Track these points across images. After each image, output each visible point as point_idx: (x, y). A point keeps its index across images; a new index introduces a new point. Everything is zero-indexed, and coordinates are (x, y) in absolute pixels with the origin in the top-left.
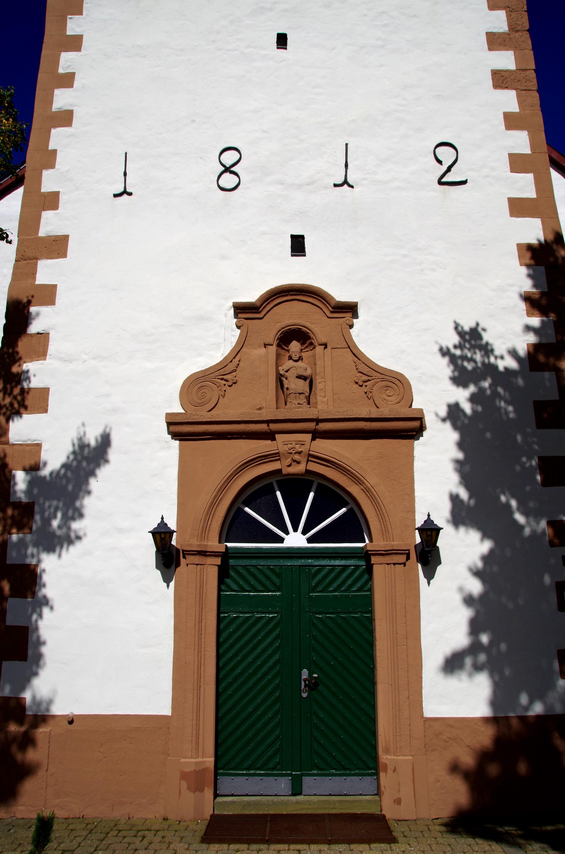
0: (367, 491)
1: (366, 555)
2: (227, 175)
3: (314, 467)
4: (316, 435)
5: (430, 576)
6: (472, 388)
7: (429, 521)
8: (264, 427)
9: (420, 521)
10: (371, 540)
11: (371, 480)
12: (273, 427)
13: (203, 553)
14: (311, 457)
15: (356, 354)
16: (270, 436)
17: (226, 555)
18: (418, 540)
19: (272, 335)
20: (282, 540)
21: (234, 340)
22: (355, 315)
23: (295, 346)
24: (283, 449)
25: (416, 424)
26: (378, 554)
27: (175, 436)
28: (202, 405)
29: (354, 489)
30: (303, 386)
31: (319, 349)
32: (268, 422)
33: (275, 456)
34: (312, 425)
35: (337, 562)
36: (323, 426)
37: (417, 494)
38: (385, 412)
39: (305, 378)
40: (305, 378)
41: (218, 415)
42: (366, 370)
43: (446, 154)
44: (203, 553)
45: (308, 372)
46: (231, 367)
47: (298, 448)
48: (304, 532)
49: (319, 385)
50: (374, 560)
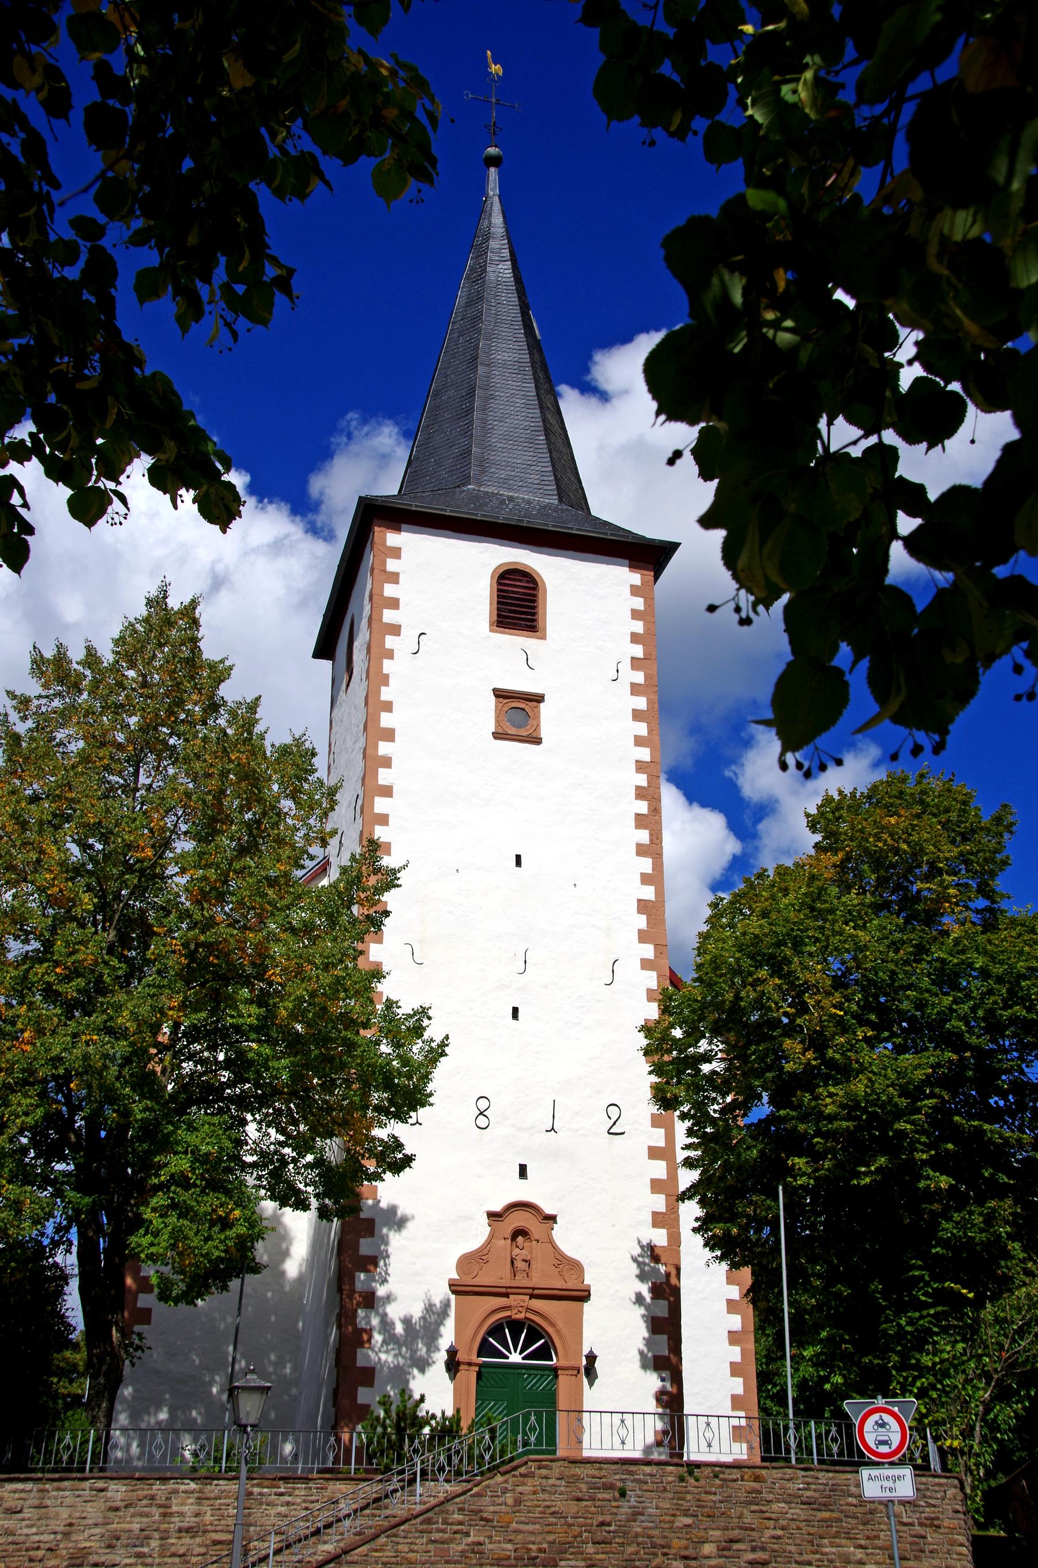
0: (558, 1331)
1: (555, 1370)
2: (481, 1117)
3: (529, 1315)
4: (532, 1296)
7: (591, 1352)
8: (504, 1290)
9: (586, 1351)
10: (558, 1360)
11: (560, 1325)
12: (509, 1290)
14: (528, 1309)
15: (555, 1247)
16: (507, 1295)
18: (584, 1362)
19: (508, 1233)
20: (508, 1358)
21: (487, 1233)
23: (520, 1239)
24: (513, 1304)
27: (454, 1292)
28: (469, 1274)
30: (525, 1265)
31: (534, 1243)
32: (507, 1288)
34: (530, 1291)
35: (532, 1372)
36: (537, 1292)
37: (585, 1335)
38: (570, 1285)
39: (526, 1261)
40: (526, 1261)
41: (478, 1281)
42: (560, 1258)
43: (614, 1112)
44: (470, 1364)
45: (528, 1258)
46: (486, 1251)
47: (522, 1304)
48: (520, 1354)
49: (533, 1265)
50: (560, 1372)
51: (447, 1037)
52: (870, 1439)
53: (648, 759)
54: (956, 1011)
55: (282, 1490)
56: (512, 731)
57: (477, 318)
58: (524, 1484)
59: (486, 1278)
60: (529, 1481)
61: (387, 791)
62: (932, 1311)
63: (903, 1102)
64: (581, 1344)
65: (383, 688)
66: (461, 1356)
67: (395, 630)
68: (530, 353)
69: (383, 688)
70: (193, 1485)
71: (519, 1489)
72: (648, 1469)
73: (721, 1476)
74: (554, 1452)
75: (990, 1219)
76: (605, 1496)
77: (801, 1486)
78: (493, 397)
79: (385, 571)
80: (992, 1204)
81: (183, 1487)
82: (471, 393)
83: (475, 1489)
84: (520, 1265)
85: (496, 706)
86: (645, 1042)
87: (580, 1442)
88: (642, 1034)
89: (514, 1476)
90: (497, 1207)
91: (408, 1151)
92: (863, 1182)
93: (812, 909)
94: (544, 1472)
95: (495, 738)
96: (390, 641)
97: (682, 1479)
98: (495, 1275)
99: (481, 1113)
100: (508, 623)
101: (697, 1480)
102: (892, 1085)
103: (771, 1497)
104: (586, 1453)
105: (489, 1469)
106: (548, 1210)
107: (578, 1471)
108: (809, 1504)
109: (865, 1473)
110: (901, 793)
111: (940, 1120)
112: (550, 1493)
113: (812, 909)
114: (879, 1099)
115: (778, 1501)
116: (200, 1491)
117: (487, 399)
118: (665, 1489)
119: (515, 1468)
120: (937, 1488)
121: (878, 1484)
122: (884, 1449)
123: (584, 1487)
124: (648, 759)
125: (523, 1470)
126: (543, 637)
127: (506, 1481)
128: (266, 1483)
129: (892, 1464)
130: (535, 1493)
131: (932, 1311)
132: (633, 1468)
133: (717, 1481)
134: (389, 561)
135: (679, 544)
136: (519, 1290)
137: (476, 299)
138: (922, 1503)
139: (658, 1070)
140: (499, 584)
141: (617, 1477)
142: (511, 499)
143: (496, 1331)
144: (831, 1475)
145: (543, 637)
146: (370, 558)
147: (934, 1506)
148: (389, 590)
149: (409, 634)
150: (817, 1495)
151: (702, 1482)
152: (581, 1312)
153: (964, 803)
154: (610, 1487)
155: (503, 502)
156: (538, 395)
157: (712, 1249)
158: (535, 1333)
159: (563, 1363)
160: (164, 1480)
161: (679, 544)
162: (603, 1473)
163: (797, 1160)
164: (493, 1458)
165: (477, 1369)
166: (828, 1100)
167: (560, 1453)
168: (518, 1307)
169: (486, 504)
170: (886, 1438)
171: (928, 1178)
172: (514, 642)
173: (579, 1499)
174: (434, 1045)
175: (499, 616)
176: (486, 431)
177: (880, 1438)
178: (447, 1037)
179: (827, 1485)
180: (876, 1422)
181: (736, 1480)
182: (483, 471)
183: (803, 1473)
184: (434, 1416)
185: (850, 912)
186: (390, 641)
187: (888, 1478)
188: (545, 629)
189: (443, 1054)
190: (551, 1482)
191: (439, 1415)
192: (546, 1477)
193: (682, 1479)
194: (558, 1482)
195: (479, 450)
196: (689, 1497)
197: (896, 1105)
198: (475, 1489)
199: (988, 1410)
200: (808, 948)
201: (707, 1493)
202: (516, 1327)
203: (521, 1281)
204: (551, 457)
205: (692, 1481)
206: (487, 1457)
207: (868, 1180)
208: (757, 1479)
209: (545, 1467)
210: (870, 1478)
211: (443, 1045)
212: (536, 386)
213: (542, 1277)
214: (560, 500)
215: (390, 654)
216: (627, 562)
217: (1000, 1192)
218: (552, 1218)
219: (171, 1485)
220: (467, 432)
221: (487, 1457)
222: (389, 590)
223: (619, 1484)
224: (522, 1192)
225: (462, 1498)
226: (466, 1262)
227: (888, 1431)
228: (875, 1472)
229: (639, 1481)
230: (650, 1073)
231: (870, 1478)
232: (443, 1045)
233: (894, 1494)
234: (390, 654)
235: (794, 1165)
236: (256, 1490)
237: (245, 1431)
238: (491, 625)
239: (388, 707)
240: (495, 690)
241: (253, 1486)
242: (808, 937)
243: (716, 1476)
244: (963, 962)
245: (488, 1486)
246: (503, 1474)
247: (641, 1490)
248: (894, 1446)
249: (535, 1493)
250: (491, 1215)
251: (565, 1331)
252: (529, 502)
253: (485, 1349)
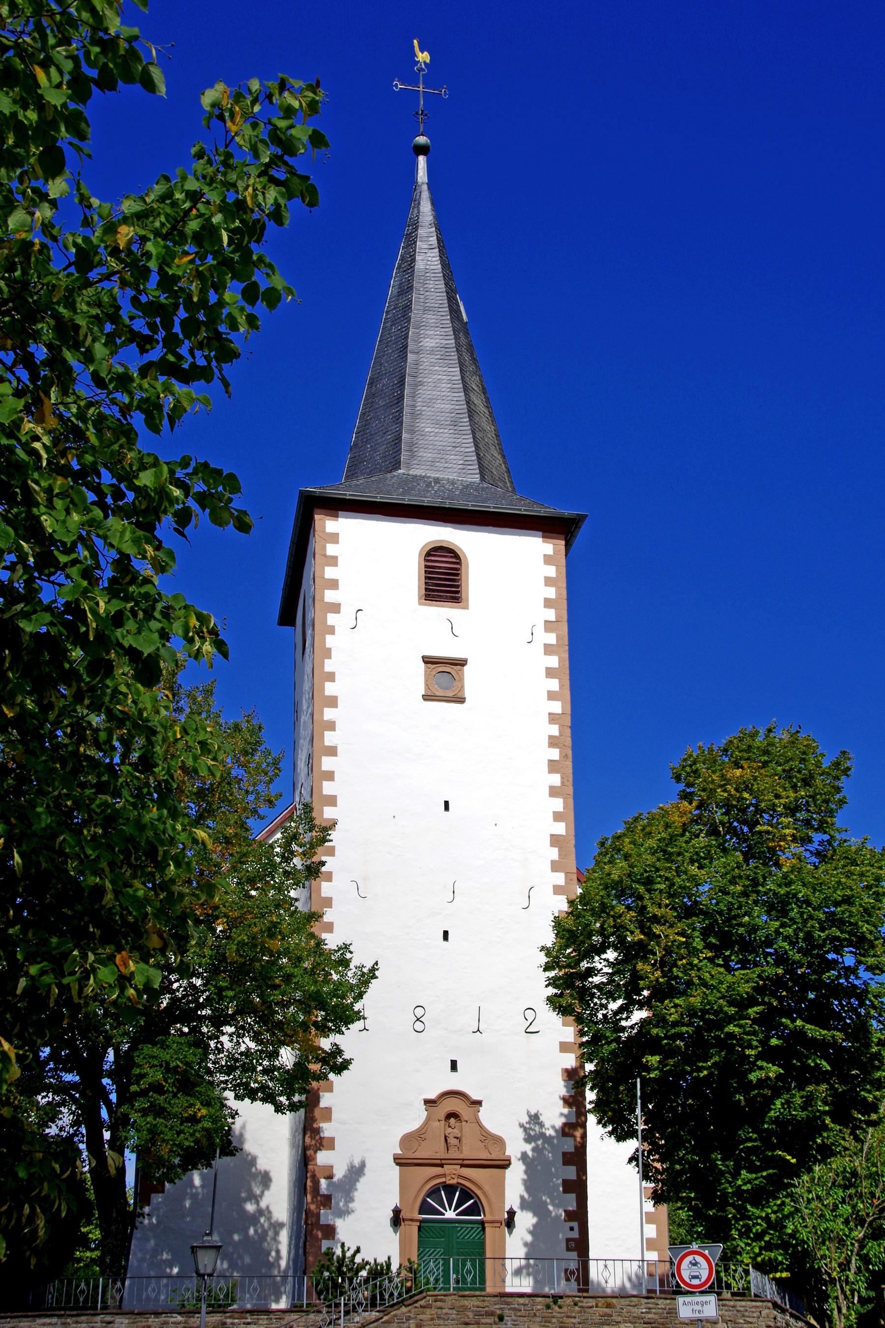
0: (484, 1193)
1: (482, 1223)
4: (462, 1166)
5: (510, 1233)
6: (533, 1144)
7: (511, 1208)
8: (439, 1162)
9: (507, 1208)
10: (485, 1215)
11: (486, 1188)
12: (443, 1162)
13: (412, 1220)
14: (460, 1176)
15: (481, 1126)
16: (442, 1166)
17: (422, 1221)
18: (506, 1216)
19: (443, 1117)
20: (444, 1214)
21: (425, 1117)
22: (481, 1106)
24: (447, 1172)
25: (507, 1162)
26: (489, 1222)
27: (397, 1164)
29: (478, 1192)
30: (456, 1141)
31: (464, 1123)
33: (444, 1175)
34: (460, 1162)
36: (466, 1162)
37: (506, 1195)
38: (494, 1157)
41: (418, 1155)
42: (485, 1134)
44: (412, 1220)
45: (459, 1135)
46: (423, 1131)
49: (464, 1141)
50: (486, 1225)
51: (376, 963)
52: (686, 1275)
54: (782, 933)
55: (249, 1320)
57: (408, 308)
58: (423, 1313)
59: (424, 1152)
60: (428, 1311)
61: (332, 751)
62: (764, 1174)
63: (732, 1010)
64: (504, 1203)
65: (326, 661)
66: (403, 1215)
67: (336, 608)
68: (456, 338)
69: (326, 661)
70: (179, 1318)
71: (420, 1317)
72: (521, 1300)
73: (580, 1304)
74: (484, 1289)
75: (809, 1101)
76: (488, 1321)
77: (644, 1310)
78: (421, 383)
79: (325, 555)
80: (810, 1088)
81: (172, 1320)
82: (402, 382)
83: (385, 1318)
84: (452, 1141)
85: (426, 671)
86: (546, 960)
87: (504, 1281)
88: (543, 953)
89: (416, 1307)
90: (432, 1096)
91: (347, 1056)
92: (702, 1075)
93: (665, 852)
94: (439, 1304)
97: (548, 1307)
98: (433, 1149)
99: (418, 1020)
100: (434, 596)
101: (560, 1307)
102: (723, 997)
103: (620, 1319)
104: (508, 1290)
105: (398, 1303)
106: (475, 1097)
107: (466, 1303)
108: (650, 1323)
109: (681, 1299)
110: (749, 746)
111: (767, 1021)
112: (444, 1319)
113: (665, 852)
114: (712, 1008)
115: (625, 1322)
116: (186, 1322)
117: (416, 385)
118: (535, 1315)
119: (417, 1301)
120: (753, 1310)
121: (690, 1308)
122: (695, 1282)
123: (471, 1315)
125: (422, 1303)
127: (409, 1311)
128: (236, 1315)
129: (702, 1292)
130: (432, 1319)
131: (764, 1174)
132: (509, 1300)
133: (577, 1308)
136: (452, 1161)
137: (406, 289)
138: (741, 1321)
139: (552, 982)
140: (426, 560)
141: (497, 1306)
142: (437, 481)
143: (434, 1193)
144: (668, 1301)
146: (316, 542)
147: (751, 1323)
148: (330, 573)
149: (348, 611)
150: (656, 1317)
151: (565, 1309)
152: (504, 1178)
153: (804, 753)
154: (491, 1314)
155: (429, 485)
156: (463, 378)
157: (604, 1126)
158: (466, 1195)
159: (488, 1218)
160: (157, 1314)
162: (486, 1304)
163: (650, 1058)
164: (400, 1295)
165: (418, 1224)
166: (673, 1010)
167: (489, 1290)
168: (452, 1174)
169: (413, 489)
170: (697, 1274)
171: (761, 1068)
173: (467, 1324)
174: (365, 970)
175: (426, 589)
176: (415, 416)
177: (692, 1274)
178: (376, 963)
179: (665, 1309)
180: (691, 1262)
181: (591, 1307)
182: (413, 456)
183: (646, 1301)
184: (368, 1263)
185: (697, 853)
187: (697, 1303)
189: (374, 977)
190: (444, 1311)
191: (372, 1262)
192: (441, 1308)
193: (548, 1307)
194: (450, 1311)
195: (408, 436)
196: (554, 1320)
197: (726, 1013)
198: (385, 1318)
199: (862, 1247)
200: (659, 886)
201: (568, 1317)
202: (450, 1189)
203: (454, 1154)
204: (474, 437)
205: (556, 1308)
206: (396, 1294)
207: (705, 1072)
208: (609, 1306)
209: (440, 1300)
210: (685, 1303)
211: (373, 970)
212: (461, 370)
213: (472, 1150)
214: (483, 478)
215: (332, 630)
217: (819, 1076)
218: (479, 1103)
219: (163, 1318)
220: (398, 419)
221: (396, 1294)
222: (330, 573)
223: (498, 1312)
224: (453, 1082)
225: (375, 1324)
226: (407, 1140)
227: (699, 1268)
228: (688, 1299)
229: (515, 1309)
230: (547, 986)
231: (685, 1303)
232: (373, 970)
233: (702, 1315)
234: (332, 630)
235: (647, 1061)
236: (229, 1321)
237: (204, 1279)
238: (420, 598)
240: (423, 657)
241: (226, 1318)
242: (660, 876)
243: (576, 1304)
244: (788, 893)
245: (395, 1316)
246: (406, 1306)
247: (515, 1315)
248: (703, 1280)
249: (432, 1319)
250: (427, 1102)
251: (491, 1193)
252: (453, 483)
253: (425, 1208)
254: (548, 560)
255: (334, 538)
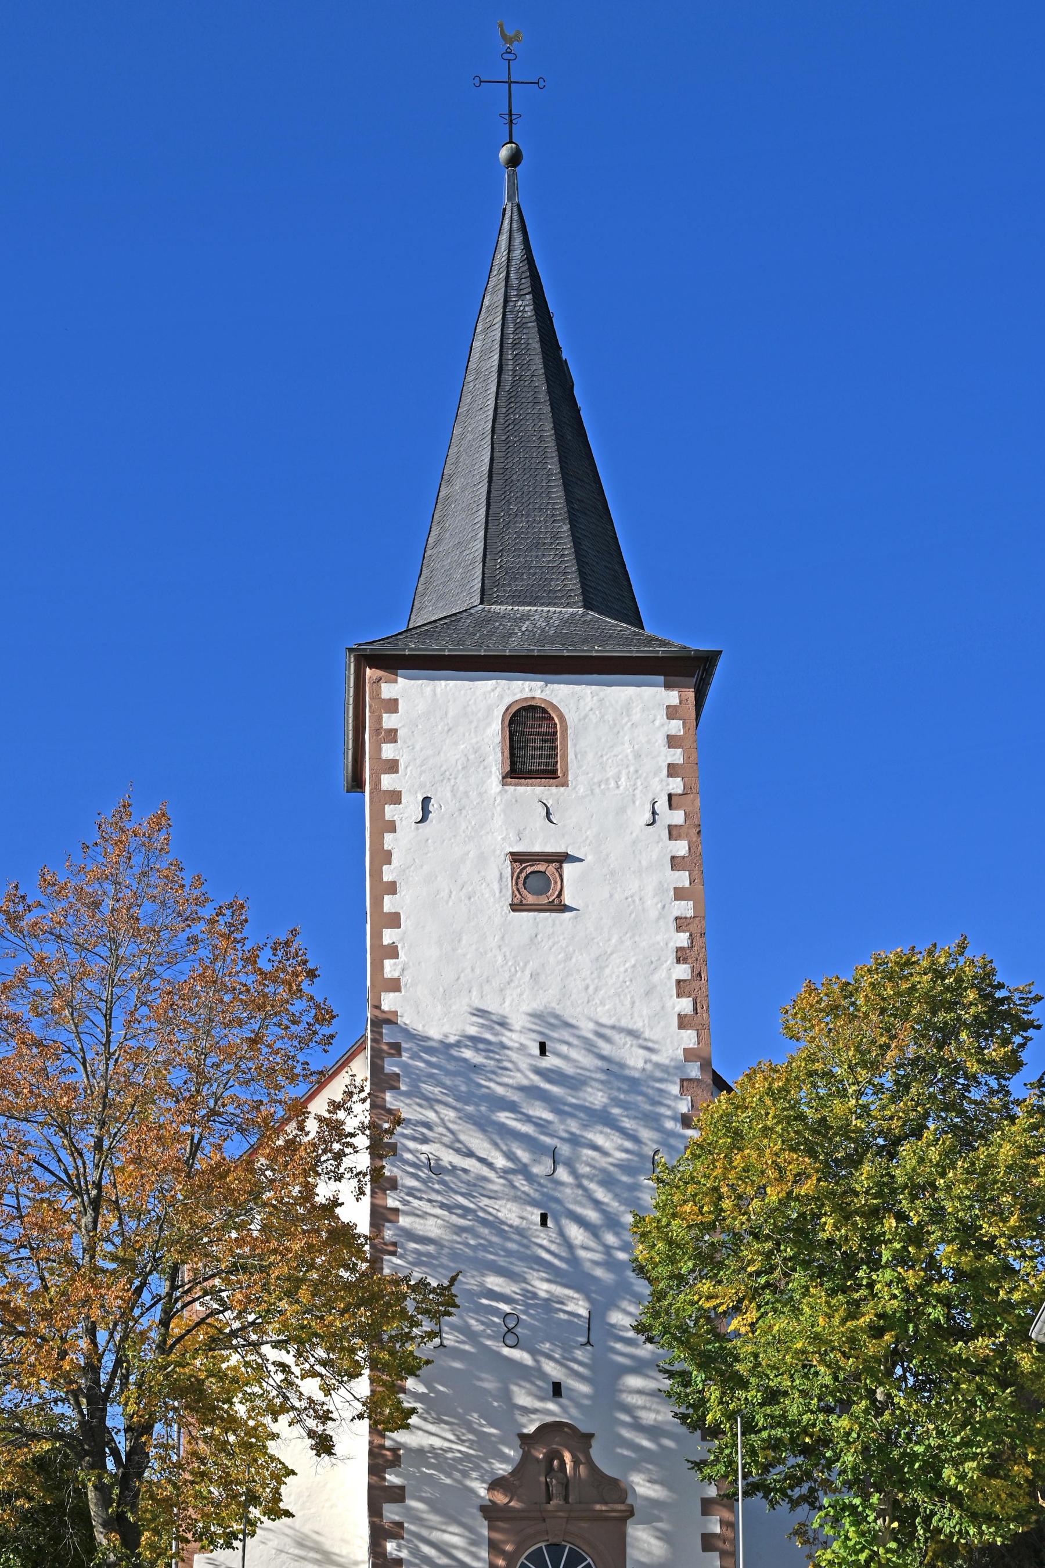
53: (690, 913)
56: (531, 899)
65: (385, 867)
69: (385, 867)
95: (514, 910)
96: (390, 812)
99: (509, 1330)
124: (690, 913)
126: (565, 784)
134: (385, 716)
135: (719, 653)
145: (565, 784)
161: (719, 653)
172: (531, 792)
186: (390, 812)
188: (565, 773)
215: (392, 827)
216: (661, 679)
234: (392, 827)
239: (392, 888)
254: (672, 713)
255: (392, 705)
